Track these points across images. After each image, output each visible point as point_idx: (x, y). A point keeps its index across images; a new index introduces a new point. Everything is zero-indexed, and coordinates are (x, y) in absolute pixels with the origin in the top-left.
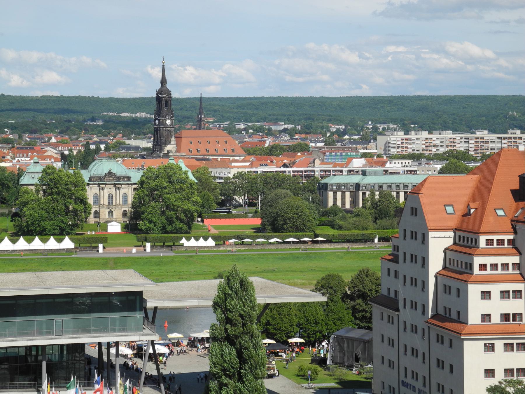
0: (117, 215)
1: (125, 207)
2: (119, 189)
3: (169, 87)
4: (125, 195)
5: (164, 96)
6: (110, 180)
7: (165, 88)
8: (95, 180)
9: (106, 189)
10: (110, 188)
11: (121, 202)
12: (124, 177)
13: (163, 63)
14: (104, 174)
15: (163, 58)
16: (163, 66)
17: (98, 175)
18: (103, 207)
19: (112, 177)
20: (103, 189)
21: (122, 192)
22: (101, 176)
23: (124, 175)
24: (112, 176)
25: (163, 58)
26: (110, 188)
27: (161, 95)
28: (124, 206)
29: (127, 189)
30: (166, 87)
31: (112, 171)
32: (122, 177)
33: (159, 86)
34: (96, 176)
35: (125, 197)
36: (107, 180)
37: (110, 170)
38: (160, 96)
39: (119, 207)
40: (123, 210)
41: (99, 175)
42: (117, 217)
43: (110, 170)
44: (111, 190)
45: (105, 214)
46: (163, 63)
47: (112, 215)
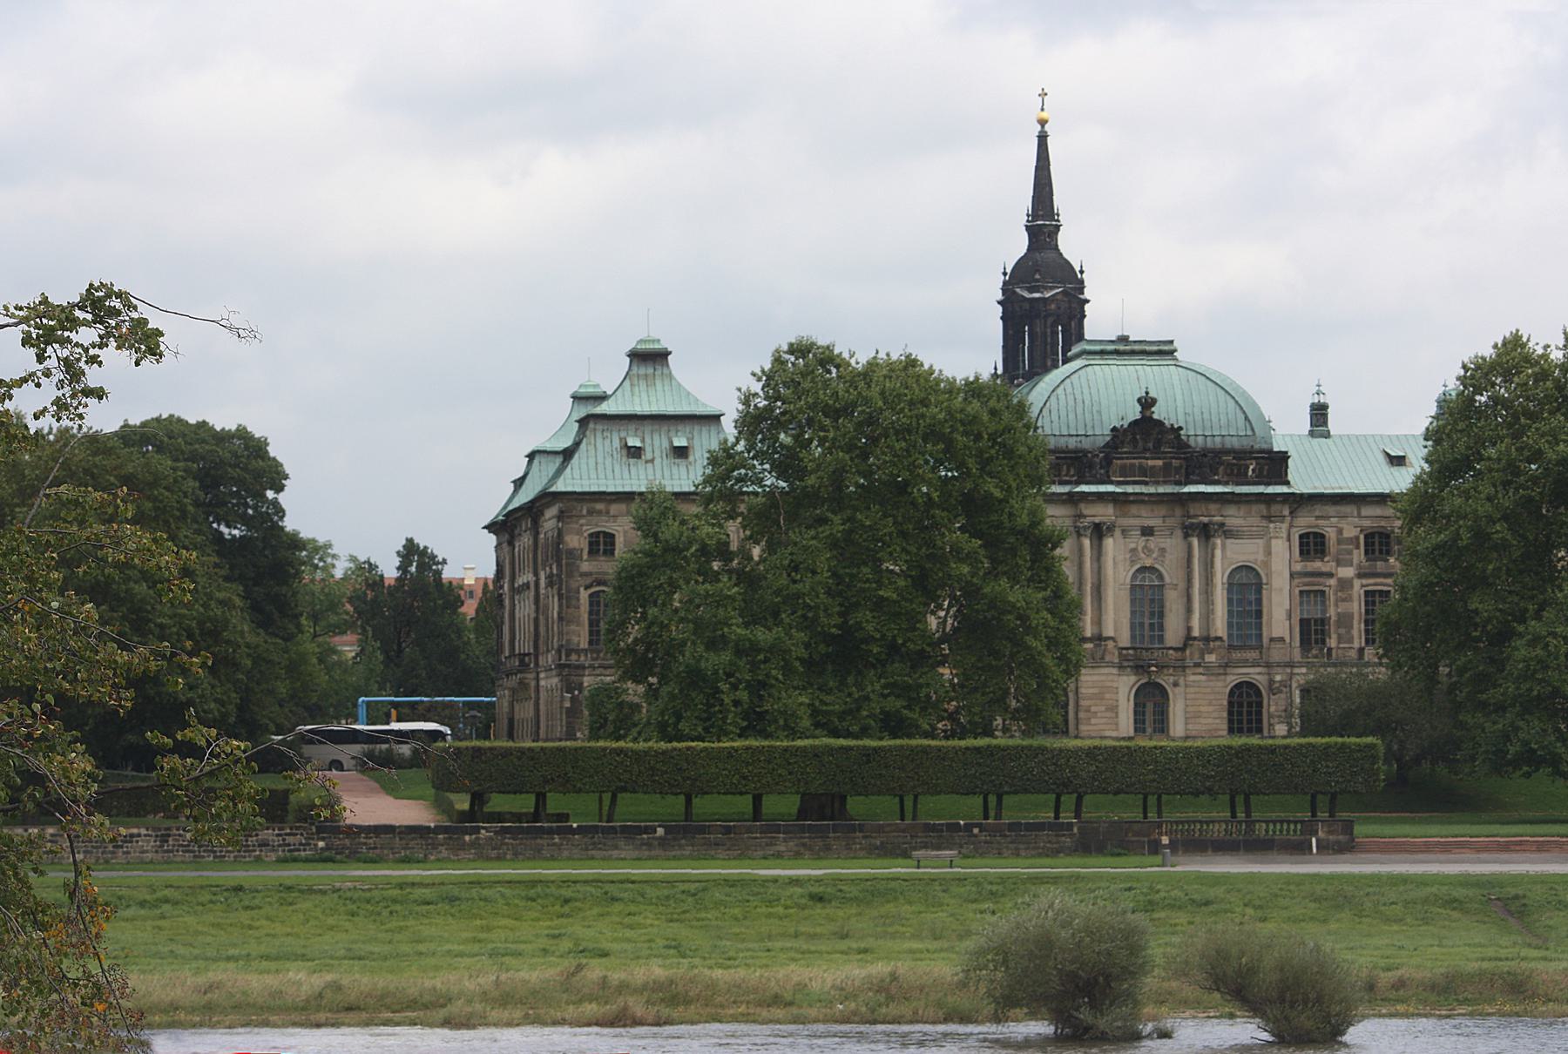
0: (1198, 715)
1: (1245, 663)
3: (1070, 245)
4: (1243, 578)
5: (1048, 295)
6: (1144, 471)
7: (1051, 255)
9: (1118, 533)
10: (1147, 532)
11: (1220, 627)
13: (1043, 123)
14: (1103, 432)
15: (1043, 94)
16: (1042, 139)
17: (1062, 442)
18: (1098, 661)
21: (1228, 555)
22: (1086, 444)
23: (1235, 443)
24: (1158, 444)
25: (1043, 94)
27: (1031, 290)
28: (1237, 655)
29: (1251, 537)
30: (1056, 248)
31: (1158, 413)
33: (1018, 245)
36: (1123, 467)
37: (1147, 403)
38: (1027, 295)
39: (1211, 658)
40: (1232, 679)
41: (1072, 443)
42: (1194, 728)
43: (1147, 403)
44: (1153, 542)
45: (1114, 709)
46: (1043, 123)
47: (1162, 725)
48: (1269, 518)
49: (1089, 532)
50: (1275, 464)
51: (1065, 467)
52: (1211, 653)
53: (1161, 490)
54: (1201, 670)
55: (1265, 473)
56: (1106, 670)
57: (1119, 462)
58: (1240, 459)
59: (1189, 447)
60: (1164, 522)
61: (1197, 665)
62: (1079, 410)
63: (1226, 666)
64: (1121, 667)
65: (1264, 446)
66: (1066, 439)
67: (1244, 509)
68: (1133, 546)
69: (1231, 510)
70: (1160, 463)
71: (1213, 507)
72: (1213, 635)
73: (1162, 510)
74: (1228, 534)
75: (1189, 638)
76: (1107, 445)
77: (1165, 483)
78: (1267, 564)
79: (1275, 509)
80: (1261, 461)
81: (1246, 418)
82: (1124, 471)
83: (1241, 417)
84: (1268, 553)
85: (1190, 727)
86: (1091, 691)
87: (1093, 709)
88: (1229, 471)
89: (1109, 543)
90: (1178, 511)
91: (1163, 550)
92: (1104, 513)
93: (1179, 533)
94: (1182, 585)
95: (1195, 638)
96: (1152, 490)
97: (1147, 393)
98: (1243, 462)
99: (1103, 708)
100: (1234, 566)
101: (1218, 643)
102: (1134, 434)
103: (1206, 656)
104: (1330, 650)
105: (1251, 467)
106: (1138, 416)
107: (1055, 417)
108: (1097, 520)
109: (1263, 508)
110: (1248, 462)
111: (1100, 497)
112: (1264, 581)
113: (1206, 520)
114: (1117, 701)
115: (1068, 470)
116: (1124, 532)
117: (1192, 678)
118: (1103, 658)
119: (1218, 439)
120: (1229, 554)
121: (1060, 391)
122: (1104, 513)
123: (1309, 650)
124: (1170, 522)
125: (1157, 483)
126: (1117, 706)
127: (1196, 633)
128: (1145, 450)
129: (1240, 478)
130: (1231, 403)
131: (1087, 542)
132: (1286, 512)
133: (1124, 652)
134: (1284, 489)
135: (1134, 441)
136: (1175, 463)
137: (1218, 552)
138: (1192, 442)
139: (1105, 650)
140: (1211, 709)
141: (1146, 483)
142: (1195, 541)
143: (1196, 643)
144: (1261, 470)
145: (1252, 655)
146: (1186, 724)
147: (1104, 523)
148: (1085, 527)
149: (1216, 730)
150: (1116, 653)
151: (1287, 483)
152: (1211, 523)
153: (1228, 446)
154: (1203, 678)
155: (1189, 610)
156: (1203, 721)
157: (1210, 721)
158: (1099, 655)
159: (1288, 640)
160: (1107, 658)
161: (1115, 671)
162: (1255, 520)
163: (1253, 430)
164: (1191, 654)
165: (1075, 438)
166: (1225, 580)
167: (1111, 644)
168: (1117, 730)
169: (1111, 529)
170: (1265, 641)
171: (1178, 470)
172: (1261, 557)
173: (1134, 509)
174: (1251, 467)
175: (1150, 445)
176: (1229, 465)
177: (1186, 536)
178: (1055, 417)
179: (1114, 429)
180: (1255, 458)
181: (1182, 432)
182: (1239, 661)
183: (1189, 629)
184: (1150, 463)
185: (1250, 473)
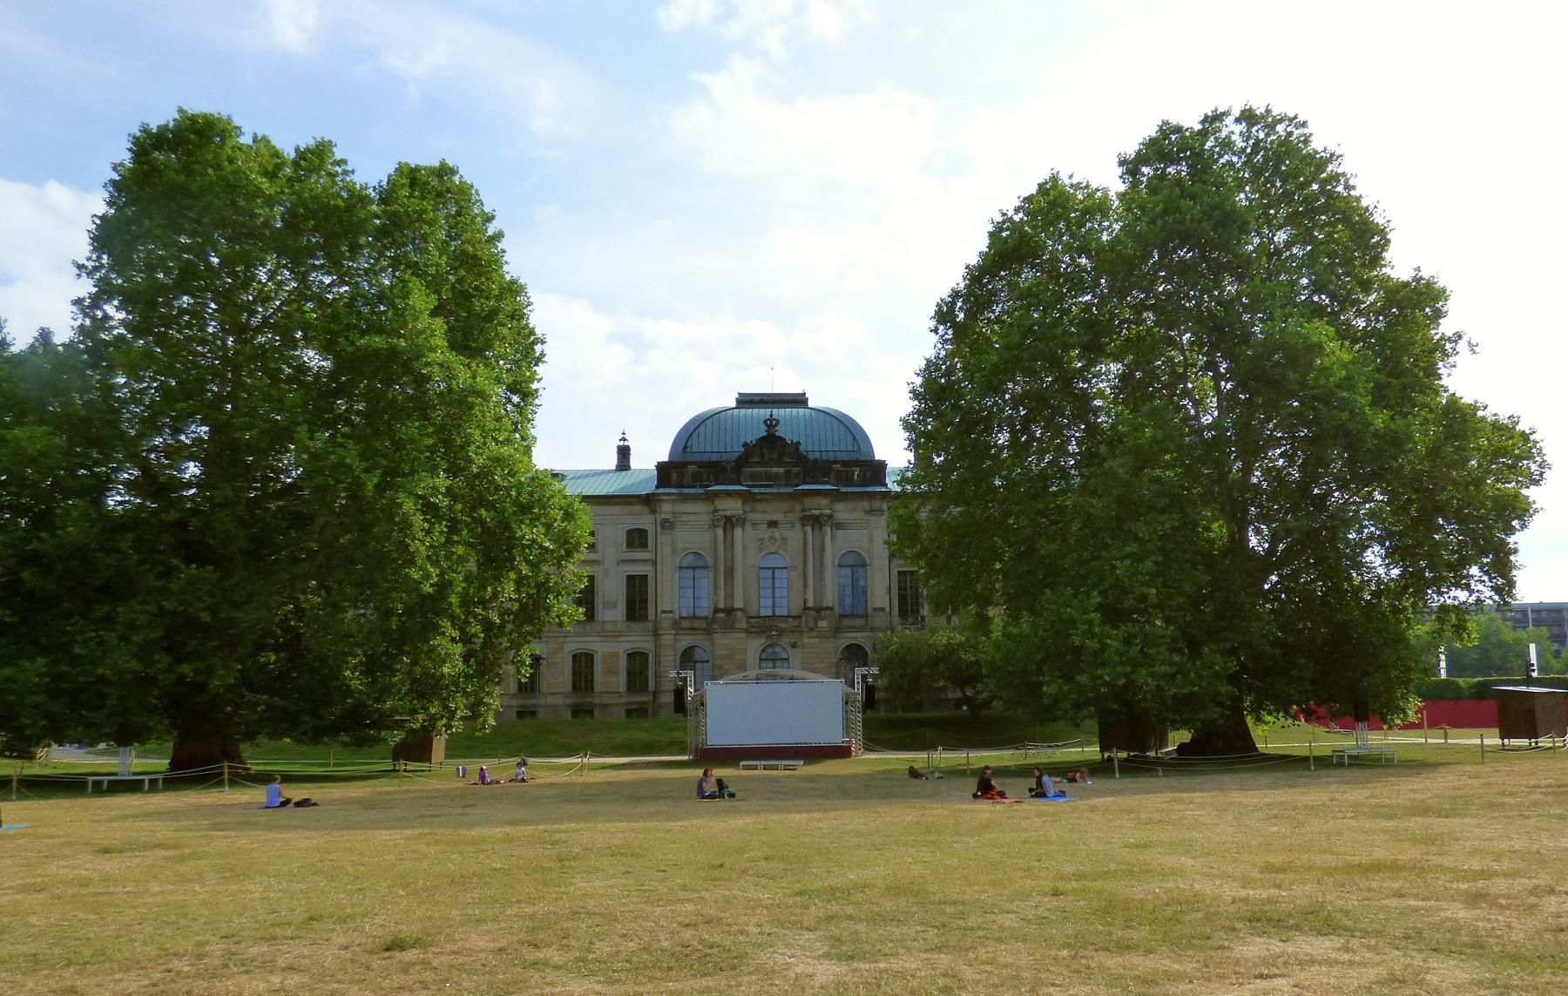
1: (853, 629)
2: (816, 522)
6: (769, 477)
8: (688, 479)
9: (748, 526)
10: (773, 524)
12: (845, 463)
17: (706, 458)
18: (730, 627)
19: (779, 463)
20: (730, 523)
21: (836, 545)
22: (725, 458)
23: (845, 456)
26: (773, 524)
28: (847, 622)
31: (781, 431)
32: (836, 462)
34: (698, 458)
35: (856, 564)
36: (753, 477)
39: (823, 624)
41: (714, 458)
43: (771, 424)
44: (777, 533)
48: (872, 512)
53: (782, 490)
54: (814, 634)
55: (868, 477)
56: (739, 635)
59: (805, 457)
60: (785, 517)
61: (811, 630)
62: (722, 434)
63: (837, 630)
64: (747, 631)
65: (868, 458)
66: (708, 455)
67: (850, 505)
69: (839, 506)
70: (782, 470)
71: (824, 502)
72: (825, 605)
73: (785, 506)
74: (839, 526)
75: (806, 608)
76: (739, 458)
77: (786, 486)
79: (876, 504)
81: (854, 439)
82: (753, 477)
83: (850, 438)
84: (871, 540)
87: (726, 667)
89: (738, 531)
90: (798, 507)
91: (784, 539)
92: (733, 507)
93: (798, 526)
94: (800, 568)
95: (809, 608)
96: (774, 490)
97: (771, 415)
98: (848, 469)
100: (841, 553)
101: (828, 612)
104: (923, 618)
105: (856, 473)
106: (765, 434)
107: (702, 439)
108: (728, 513)
109: (866, 505)
110: (854, 469)
111: (729, 494)
112: (868, 563)
113: (817, 512)
115: (709, 477)
116: (754, 525)
117: (807, 641)
122: (733, 507)
123: (906, 620)
124: (791, 517)
125: (780, 486)
127: (810, 604)
129: (848, 481)
130: (842, 429)
131: (720, 531)
133: (752, 620)
136: (795, 470)
138: (811, 456)
141: (770, 486)
142: (809, 529)
144: (865, 475)
145: (859, 622)
148: (718, 520)
150: (744, 620)
152: (821, 515)
153: (839, 459)
155: (805, 586)
159: (888, 610)
160: (737, 626)
161: (743, 635)
162: (859, 515)
166: (836, 563)
167: (739, 614)
169: (741, 521)
170: (870, 611)
171: (797, 475)
173: (760, 506)
174: (856, 473)
175: (775, 456)
176: (839, 472)
177: (803, 525)
178: (702, 439)
179: (745, 445)
181: (802, 448)
182: (849, 627)
183: (805, 601)
184: (775, 470)
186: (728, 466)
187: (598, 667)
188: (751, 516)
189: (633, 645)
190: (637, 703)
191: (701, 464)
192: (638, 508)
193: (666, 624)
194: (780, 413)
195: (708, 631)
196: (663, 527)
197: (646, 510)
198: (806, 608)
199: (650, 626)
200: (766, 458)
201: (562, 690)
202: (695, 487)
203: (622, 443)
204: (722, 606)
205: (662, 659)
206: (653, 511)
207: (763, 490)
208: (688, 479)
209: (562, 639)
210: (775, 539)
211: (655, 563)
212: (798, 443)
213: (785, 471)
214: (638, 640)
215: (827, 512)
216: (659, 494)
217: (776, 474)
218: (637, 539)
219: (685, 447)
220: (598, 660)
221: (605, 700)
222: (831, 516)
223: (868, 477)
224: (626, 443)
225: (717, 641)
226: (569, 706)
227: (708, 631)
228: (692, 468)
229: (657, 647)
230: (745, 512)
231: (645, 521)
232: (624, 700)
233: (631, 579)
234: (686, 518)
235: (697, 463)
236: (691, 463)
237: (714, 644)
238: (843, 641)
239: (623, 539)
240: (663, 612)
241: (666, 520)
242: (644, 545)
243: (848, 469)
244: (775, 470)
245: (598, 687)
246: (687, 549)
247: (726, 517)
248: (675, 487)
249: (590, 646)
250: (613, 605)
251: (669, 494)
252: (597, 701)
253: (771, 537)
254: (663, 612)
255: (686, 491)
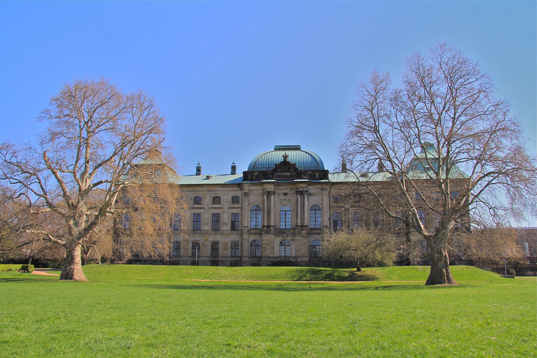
6: (284, 177)
8: (254, 178)
9: (276, 195)
10: (285, 194)
12: (313, 171)
17: (262, 170)
18: (268, 232)
20: (269, 194)
23: (313, 169)
24: (289, 168)
26: (285, 194)
28: (313, 231)
31: (289, 159)
32: (309, 171)
34: (258, 170)
41: (264, 170)
42: (298, 254)
43: (285, 157)
44: (287, 197)
45: (273, 248)
48: (322, 189)
49: (266, 194)
50: (325, 174)
51: (261, 176)
52: (303, 230)
53: (289, 181)
54: (300, 236)
55: (321, 176)
56: (271, 236)
57: (277, 174)
58: (314, 172)
60: (290, 191)
61: (299, 234)
64: (275, 234)
65: (322, 169)
66: (263, 169)
67: (315, 187)
68: (281, 199)
69: (311, 187)
70: (289, 174)
74: (310, 195)
78: (322, 204)
79: (325, 186)
80: (320, 173)
84: (323, 200)
85: (297, 253)
86: (266, 242)
87: (266, 248)
88: (310, 176)
89: (272, 197)
90: (295, 188)
93: (295, 194)
94: (295, 211)
95: (298, 226)
96: (286, 181)
97: (285, 154)
98: (314, 173)
99: (269, 248)
100: (312, 205)
101: (306, 227)
102: (281, 166)
103: (302, 231)
105: (317, 175)
106: (282, 161)
108: (268, 190)
109: (320, 186)
110: (316, 173)
111: (269, 183)
113: (302, 190)
114: (274, 245)
117: (297, 238)
118: (270, 232)
119: (308, 168)
120: (310, 201)
121: (262, 156)
122: (271, 188)
125: (288, 180)
126: (274, 247)
127: (299, 224)
128: (285, 170)
131: (266, 197)
132: (328, 187)
133: (277, 230)
134: (327, 181)
135: (282, 168)
137: (306, 200)
139: (270, 230)
140: (303, 248)
142: (299, 196)
143: (299, 227)
144: (320, 175)
146: (296, 252)
147: (270, 191)
148: (265, 193)
149: (305, 254)
150: (274, 230)
151: (328, 179)
152: (304, 191)
154: (301, 238)
155: (297, 217)
156: (301, 251)
157: (303, 251)
158: (268, 231)
159: (329, 226)
160: (271, 232)
161: (273, 236)
162: (318, 191)
163: (318, 165)
164: (297, 231)
165: (265, 169)
166: (309, 209)
167: (272, 228)
168: (274, 254)
169: (274, 193)
171: (295, 176)
172: (320, 202)
173: (281, 187)
174: (317, 175)
175: (286, 169)
176: (310, 174)
177: (297, 195)
179: (276, 165)
180: (318, 172)
183: (297, 223)
184: (286, 174)
185: (317, 176)
186: (269, 172)
187: (221, 247)
188: (277, 191)
189: (232, 239)
190: (234, 261)
191: (258, 172)
192: (236, 188)
193: (245, 231)
194: (288, 153)
195: (260, 234)
196: (245, 195)
197: (239, 189)
198: (297, 226)
199: (240, 232)
200: (284, 169)
201: (207, 255)
202: (257, 180)
203: (233, 165)
204: (266, 225)
205: (243, 244)
206: (241, 189)
207: (282, 181)
208: (254, 178)
209: (208, 236)
210: (286, 200)
211: (241, 208)
212: (295, 164)
213: (291, 174)
214: (234, 237)
215: (306, 189)
216: (243, 183)
217: (287, 175)
218: (235, 200)
219: (254, 166)
220: (221, 243)
221: (223, 259)
222: (307, 191)
223: (321, 176)
224: (235, 165)
225: (264, 238)
226: (210, 261)
227: (260, 234)
228: (256, 173)
229: (242, 240)
230: (275, 190)
231: (239, 193)
232: (229, 259)
233: (214, 215)
234: (253, 192)
235: (257, 172)
236: (256, 172)
237: (262, 239)
238: (312, 238)
239: (230, 199)
240: (244, 227)
241: (246, 193)
242: (238, 202)
243: (314, 173)
244: (286, 174)
245: (220, 255)
246: (254, 203)
247: (267, 191)
248: (250, 181)
249: (218, 239)
250: (226, 224)
251: (247, 183)
252: (220, 259)
253: (285, 199)
254: (244, 227)
255: (253, 182)
